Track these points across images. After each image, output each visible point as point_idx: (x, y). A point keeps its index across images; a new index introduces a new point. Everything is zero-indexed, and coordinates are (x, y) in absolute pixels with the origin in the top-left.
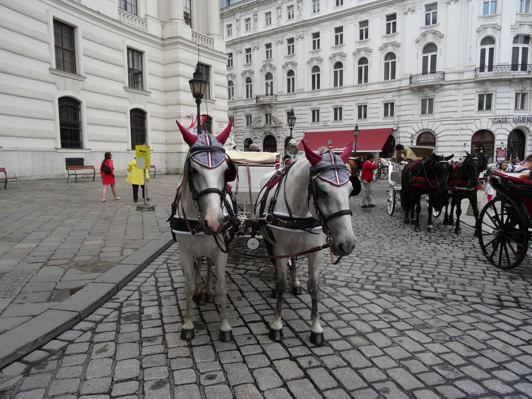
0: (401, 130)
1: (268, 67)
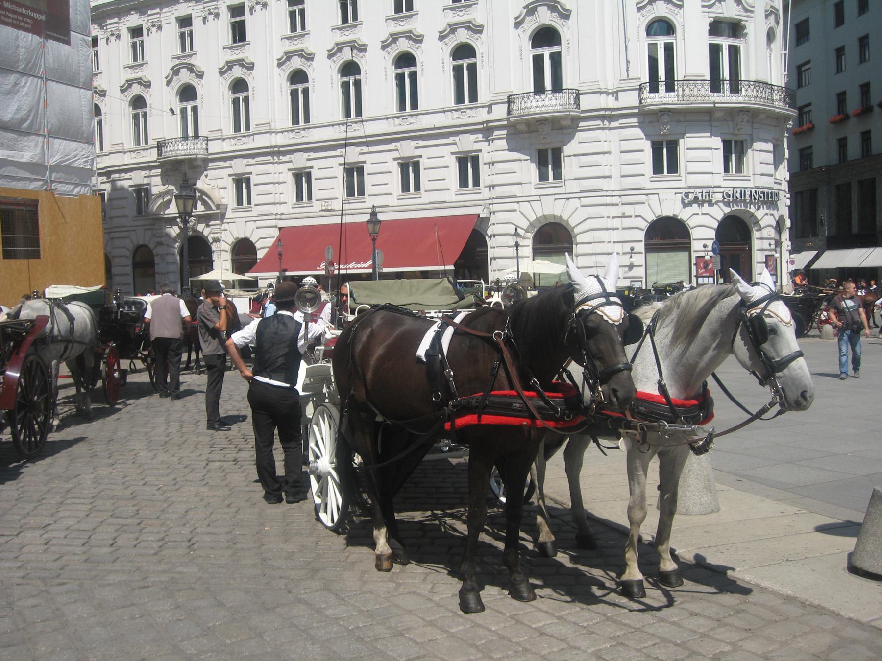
1: (184, 71)
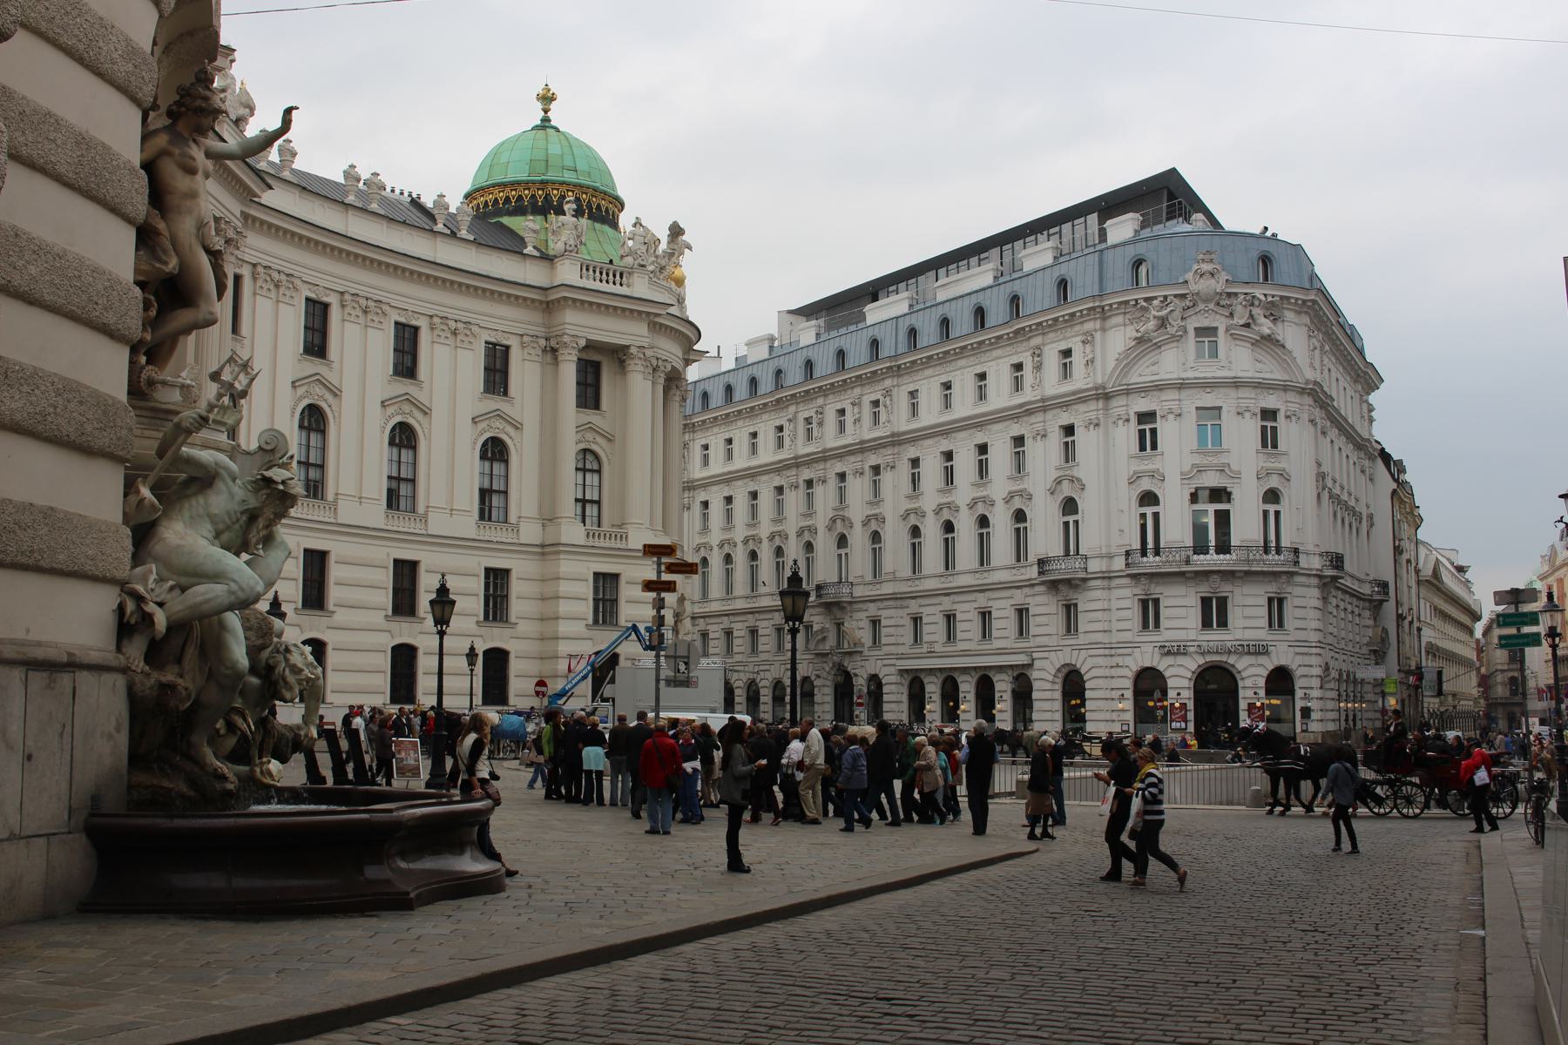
0: (1037, 664)
